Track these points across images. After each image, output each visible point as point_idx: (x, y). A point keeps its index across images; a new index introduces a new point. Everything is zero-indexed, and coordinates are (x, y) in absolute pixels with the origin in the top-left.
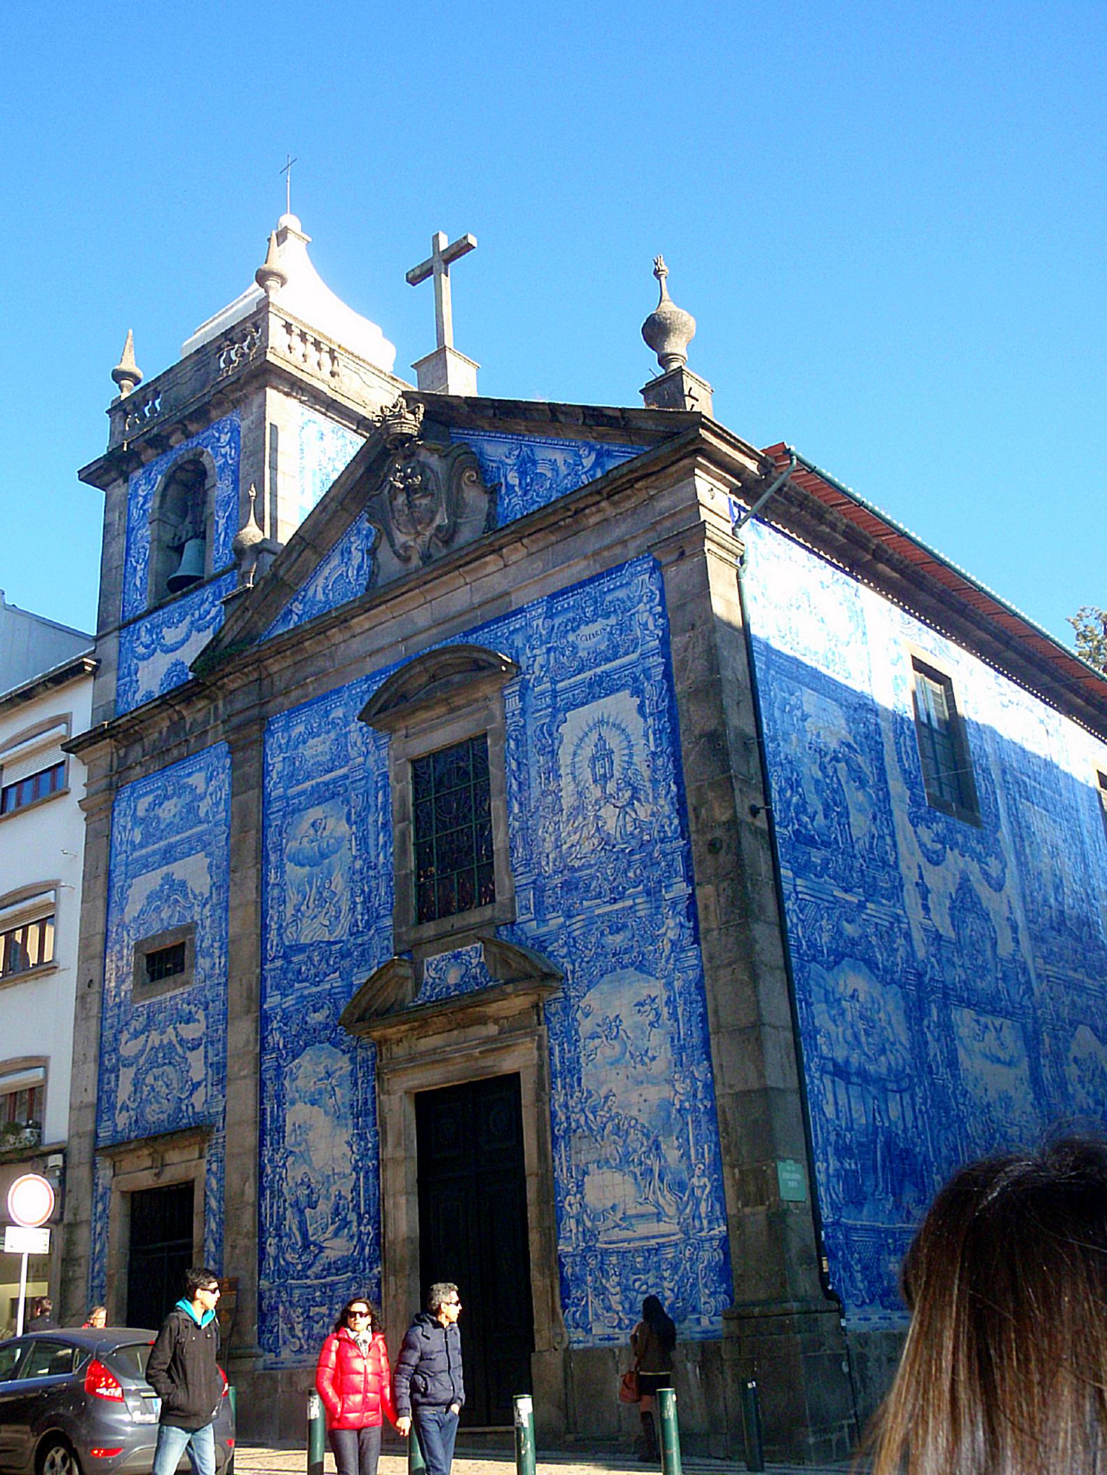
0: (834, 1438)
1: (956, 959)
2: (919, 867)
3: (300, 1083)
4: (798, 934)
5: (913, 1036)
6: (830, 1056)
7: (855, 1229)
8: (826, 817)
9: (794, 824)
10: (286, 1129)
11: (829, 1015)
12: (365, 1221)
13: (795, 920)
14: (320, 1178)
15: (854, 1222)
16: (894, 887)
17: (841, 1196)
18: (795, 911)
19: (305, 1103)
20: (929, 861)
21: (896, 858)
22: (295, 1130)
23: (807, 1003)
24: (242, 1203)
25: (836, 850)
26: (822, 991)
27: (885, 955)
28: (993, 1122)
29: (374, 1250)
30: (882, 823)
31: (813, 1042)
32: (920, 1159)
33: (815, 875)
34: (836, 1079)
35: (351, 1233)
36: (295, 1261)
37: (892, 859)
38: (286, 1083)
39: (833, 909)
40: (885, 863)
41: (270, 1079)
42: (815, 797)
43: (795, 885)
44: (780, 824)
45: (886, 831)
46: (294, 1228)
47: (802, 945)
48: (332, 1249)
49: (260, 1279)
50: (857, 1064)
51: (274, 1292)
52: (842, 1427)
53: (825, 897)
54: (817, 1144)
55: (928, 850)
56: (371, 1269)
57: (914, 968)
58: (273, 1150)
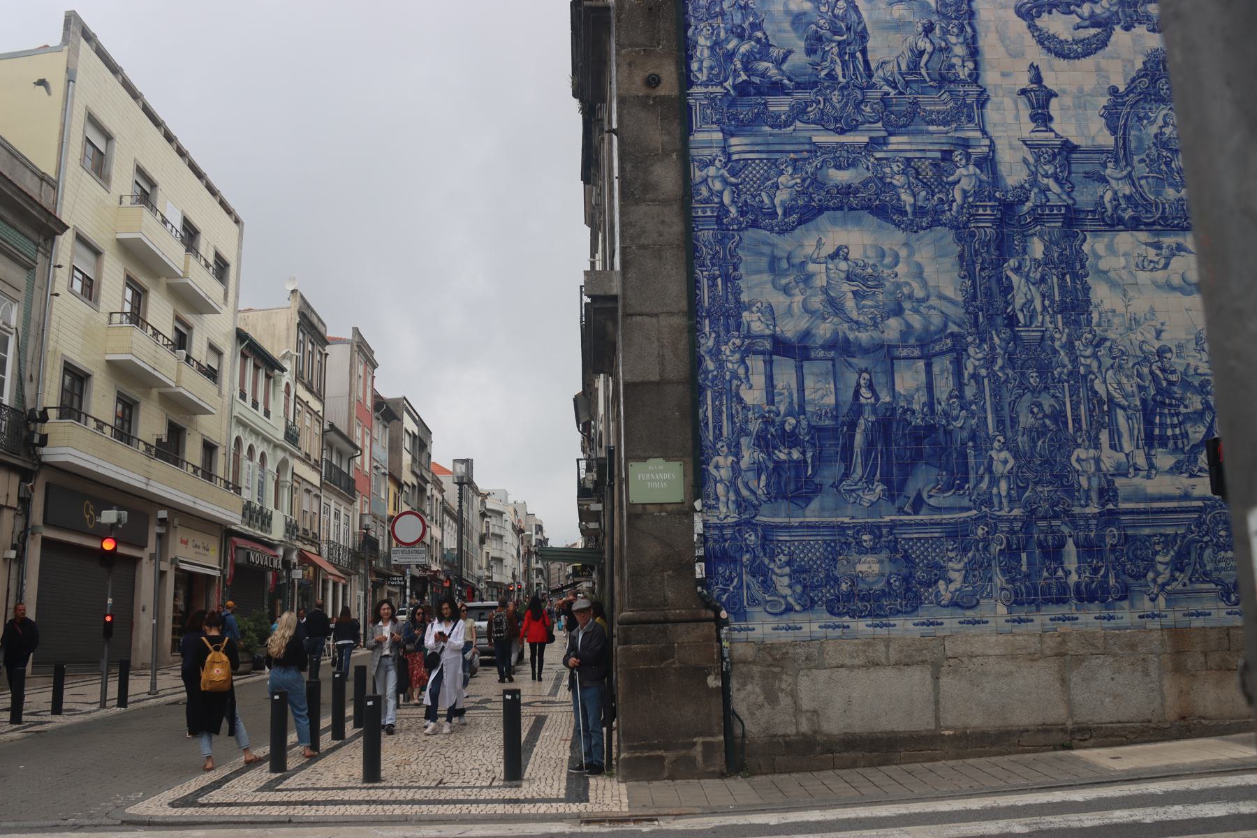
0: (670, 756)
1: (1109, 171)
2: (1035, 69)
4: (722, 203)
5: (974, 286)
6: (768, 332)
7: (788, 527)
8: (810, 51)
9: (736, 75)
11: (775, 287)
13: (718, 186)
15: (787, 520)
16: (970, 106)
17: (760, 492)
18: (722, 176)
20: (1060, 55)
21: (976, 68)
23: (727, 278)
25: (827, 88)
26: (764, 262)
27: (923, 193)
28: (1173, 372)
30: (945, 32)
31: (731, 322)
32: (965, 434)
33: (771, 126)
34: (775, 357)
37: (963, 74)
39: (805, 159)
40: (944, 80)
42: (793, 35)
43: (725, 149)
44: (705, 84)
45: (953, 39)
47: (728, 212)
50: (828, 335)
52: (695, 744)
53: (788, 148)
54: (718, 437)
55: (1061, 41)
57: (991, 197)
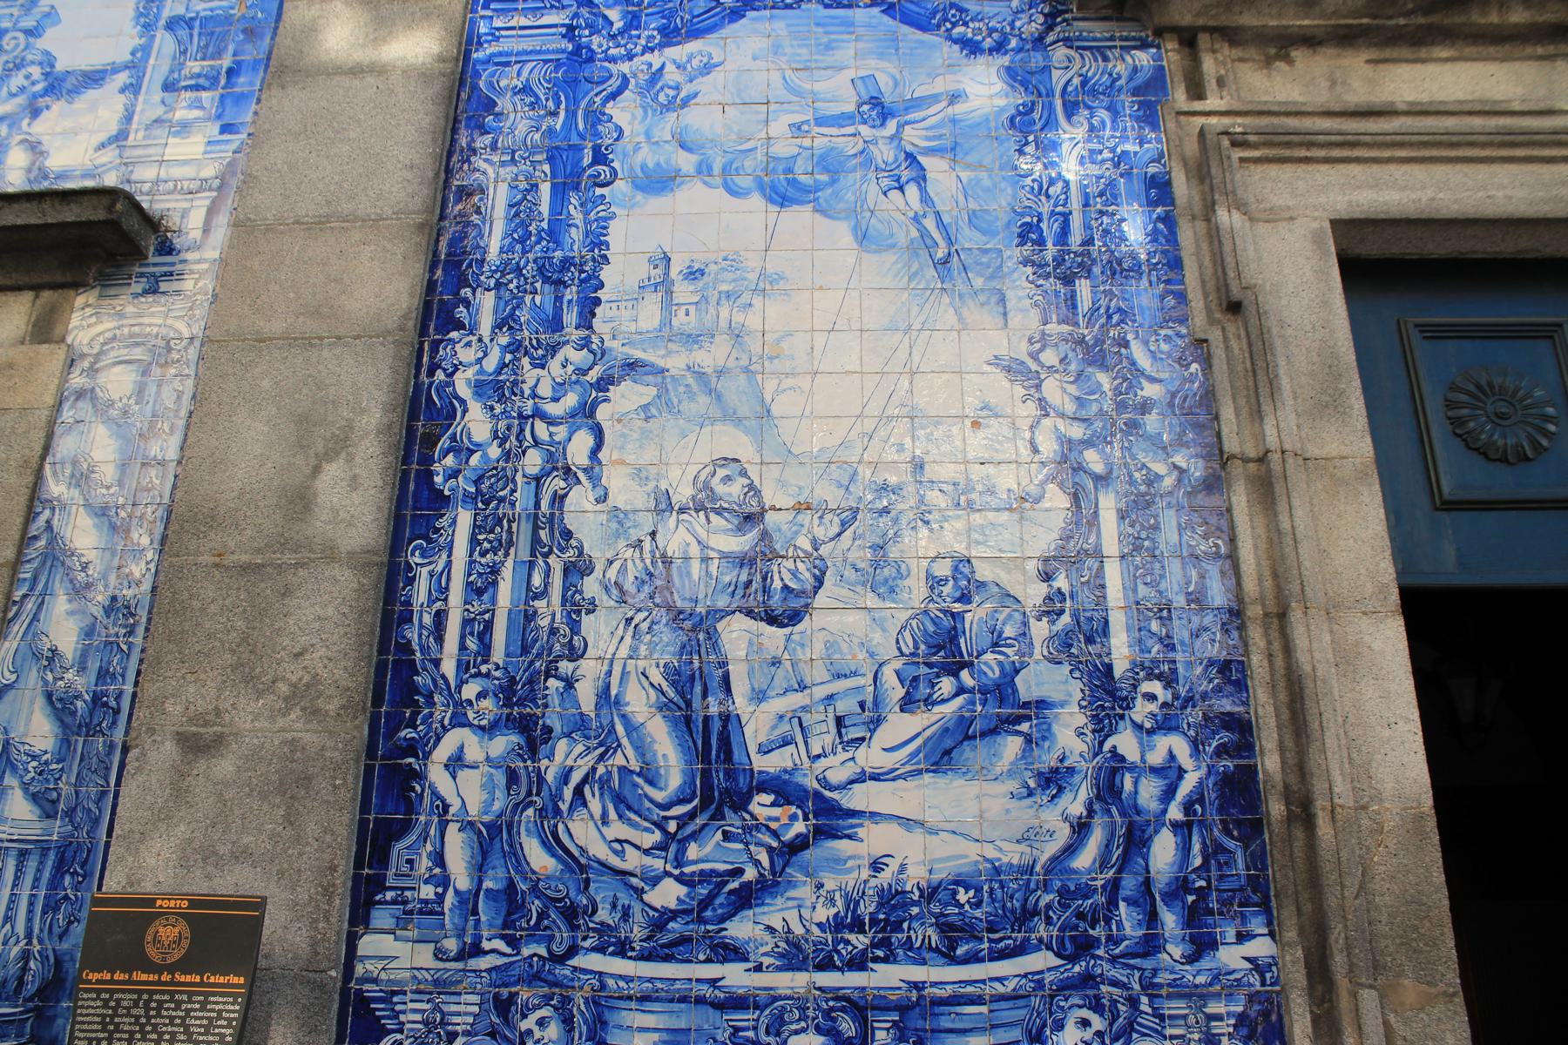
3: (698, 119)
10: (606, 274)
12: (1142, 711)
14: (828, 493)
19: (733, 191)
22: (664, 286)
24: (284, 544)
29: (1214, 852)
35: (1048, 760)
36: (633, 860)
38: (623, 113)
41: (526, 89)
46: (639, 702)
48: (906, 822)
49: (360, 916)
51: (465, 1009)
56: (1202, 945)
58: (515, 347)
